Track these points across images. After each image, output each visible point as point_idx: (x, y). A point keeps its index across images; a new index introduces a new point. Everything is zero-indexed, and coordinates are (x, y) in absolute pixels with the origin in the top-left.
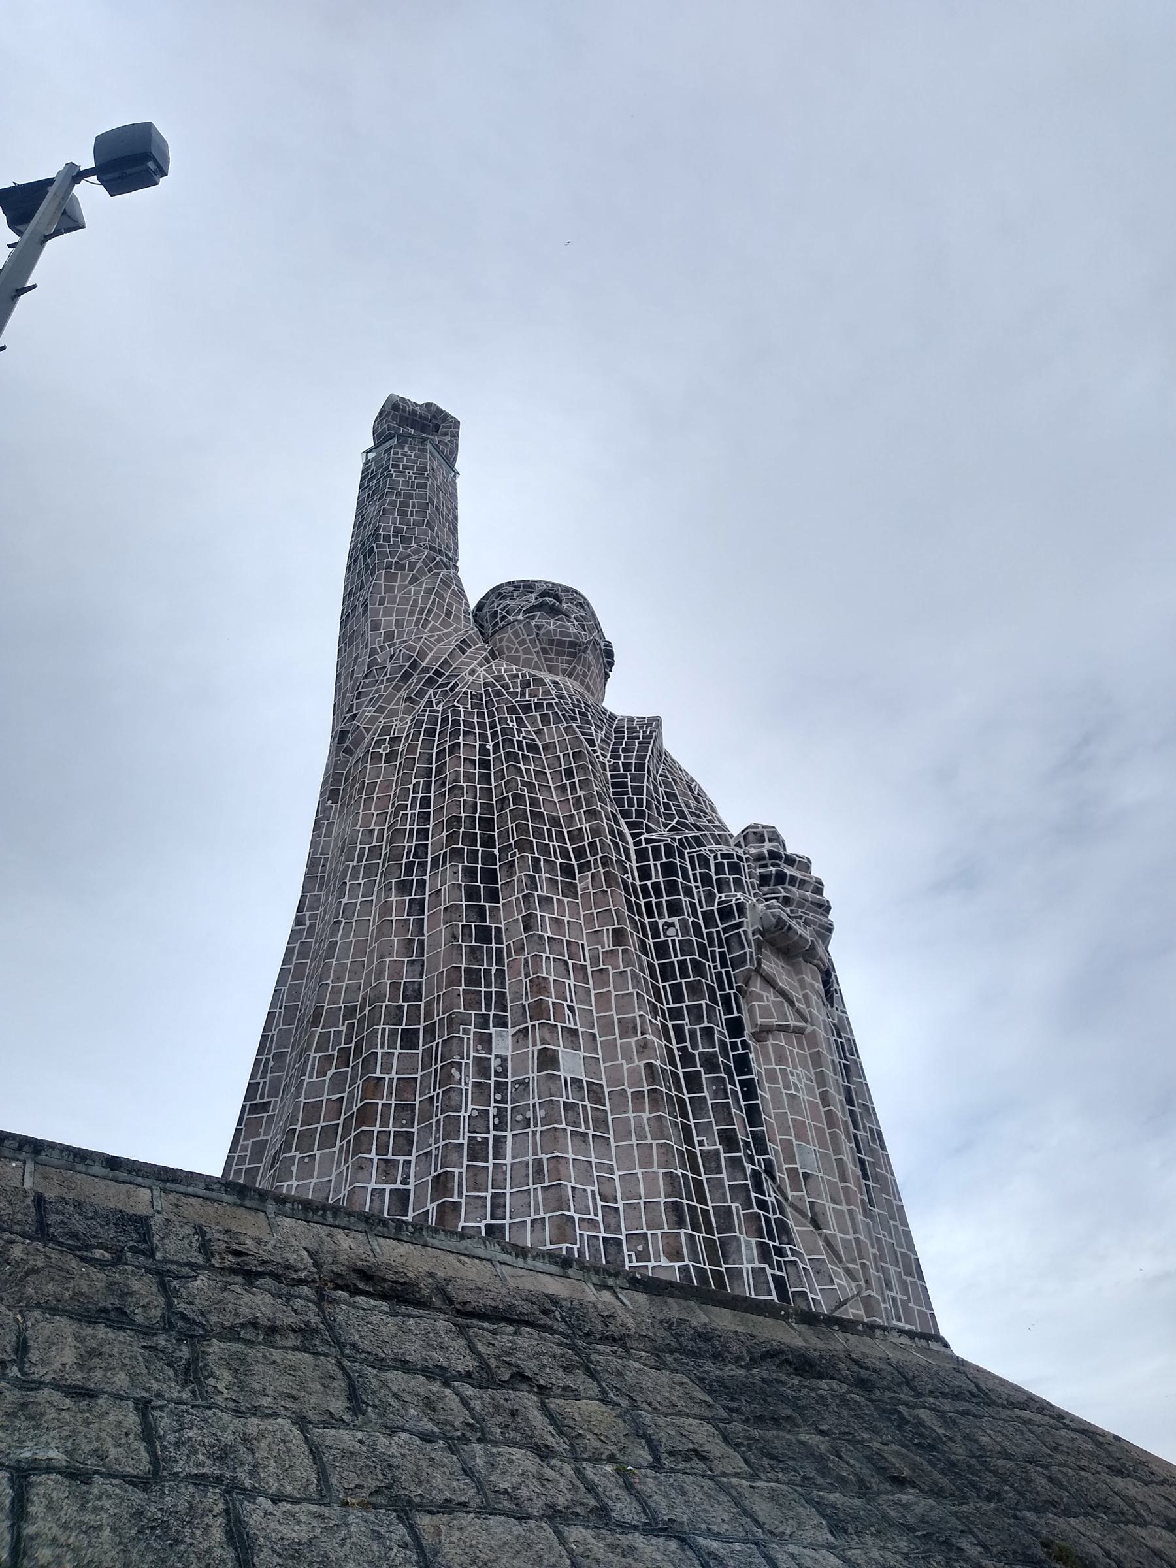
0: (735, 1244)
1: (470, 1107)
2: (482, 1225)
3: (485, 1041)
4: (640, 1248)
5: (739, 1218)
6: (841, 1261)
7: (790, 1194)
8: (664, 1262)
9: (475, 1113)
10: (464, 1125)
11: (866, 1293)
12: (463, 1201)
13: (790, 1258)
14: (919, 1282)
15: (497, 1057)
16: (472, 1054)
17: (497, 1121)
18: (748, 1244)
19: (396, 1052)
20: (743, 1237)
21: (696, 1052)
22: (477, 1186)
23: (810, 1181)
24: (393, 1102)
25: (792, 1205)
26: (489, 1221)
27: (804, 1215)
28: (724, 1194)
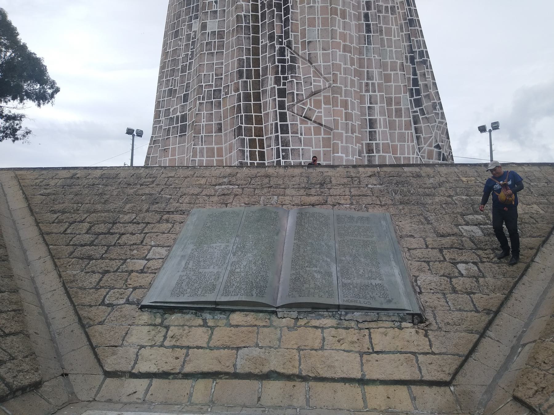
0: (267, 80)
1: (183, 54)
2: (182, 95)
3: (190, 27)
4: (226, 90)
5: (270, 70)
6: (322, 75)
7: (300, 53)
8: (233, 93)
9: (184, 55)
10: (180, 61)
11: (332, 86)
12: (178, 88)
13: (290, 80)
14: (429, 70)
15: (193, 32)
16: (186, 33)
17: (191, 56)
18: (271, 78)
19: (173, 40)
20: (270, 76)
21: (266, 2)
22: (182, 82)
23: (311, 45)
24: (171, 59)
25: (302, 57)
26: (185, 93)
27: (305, 59)
28: (266, 61)
